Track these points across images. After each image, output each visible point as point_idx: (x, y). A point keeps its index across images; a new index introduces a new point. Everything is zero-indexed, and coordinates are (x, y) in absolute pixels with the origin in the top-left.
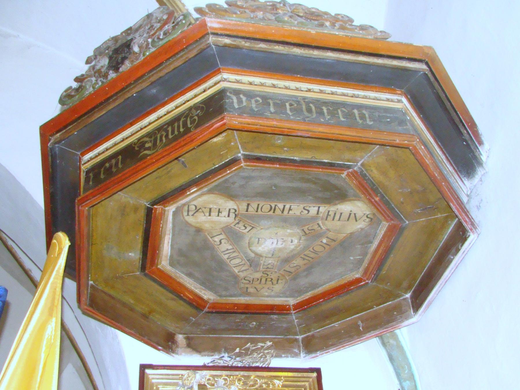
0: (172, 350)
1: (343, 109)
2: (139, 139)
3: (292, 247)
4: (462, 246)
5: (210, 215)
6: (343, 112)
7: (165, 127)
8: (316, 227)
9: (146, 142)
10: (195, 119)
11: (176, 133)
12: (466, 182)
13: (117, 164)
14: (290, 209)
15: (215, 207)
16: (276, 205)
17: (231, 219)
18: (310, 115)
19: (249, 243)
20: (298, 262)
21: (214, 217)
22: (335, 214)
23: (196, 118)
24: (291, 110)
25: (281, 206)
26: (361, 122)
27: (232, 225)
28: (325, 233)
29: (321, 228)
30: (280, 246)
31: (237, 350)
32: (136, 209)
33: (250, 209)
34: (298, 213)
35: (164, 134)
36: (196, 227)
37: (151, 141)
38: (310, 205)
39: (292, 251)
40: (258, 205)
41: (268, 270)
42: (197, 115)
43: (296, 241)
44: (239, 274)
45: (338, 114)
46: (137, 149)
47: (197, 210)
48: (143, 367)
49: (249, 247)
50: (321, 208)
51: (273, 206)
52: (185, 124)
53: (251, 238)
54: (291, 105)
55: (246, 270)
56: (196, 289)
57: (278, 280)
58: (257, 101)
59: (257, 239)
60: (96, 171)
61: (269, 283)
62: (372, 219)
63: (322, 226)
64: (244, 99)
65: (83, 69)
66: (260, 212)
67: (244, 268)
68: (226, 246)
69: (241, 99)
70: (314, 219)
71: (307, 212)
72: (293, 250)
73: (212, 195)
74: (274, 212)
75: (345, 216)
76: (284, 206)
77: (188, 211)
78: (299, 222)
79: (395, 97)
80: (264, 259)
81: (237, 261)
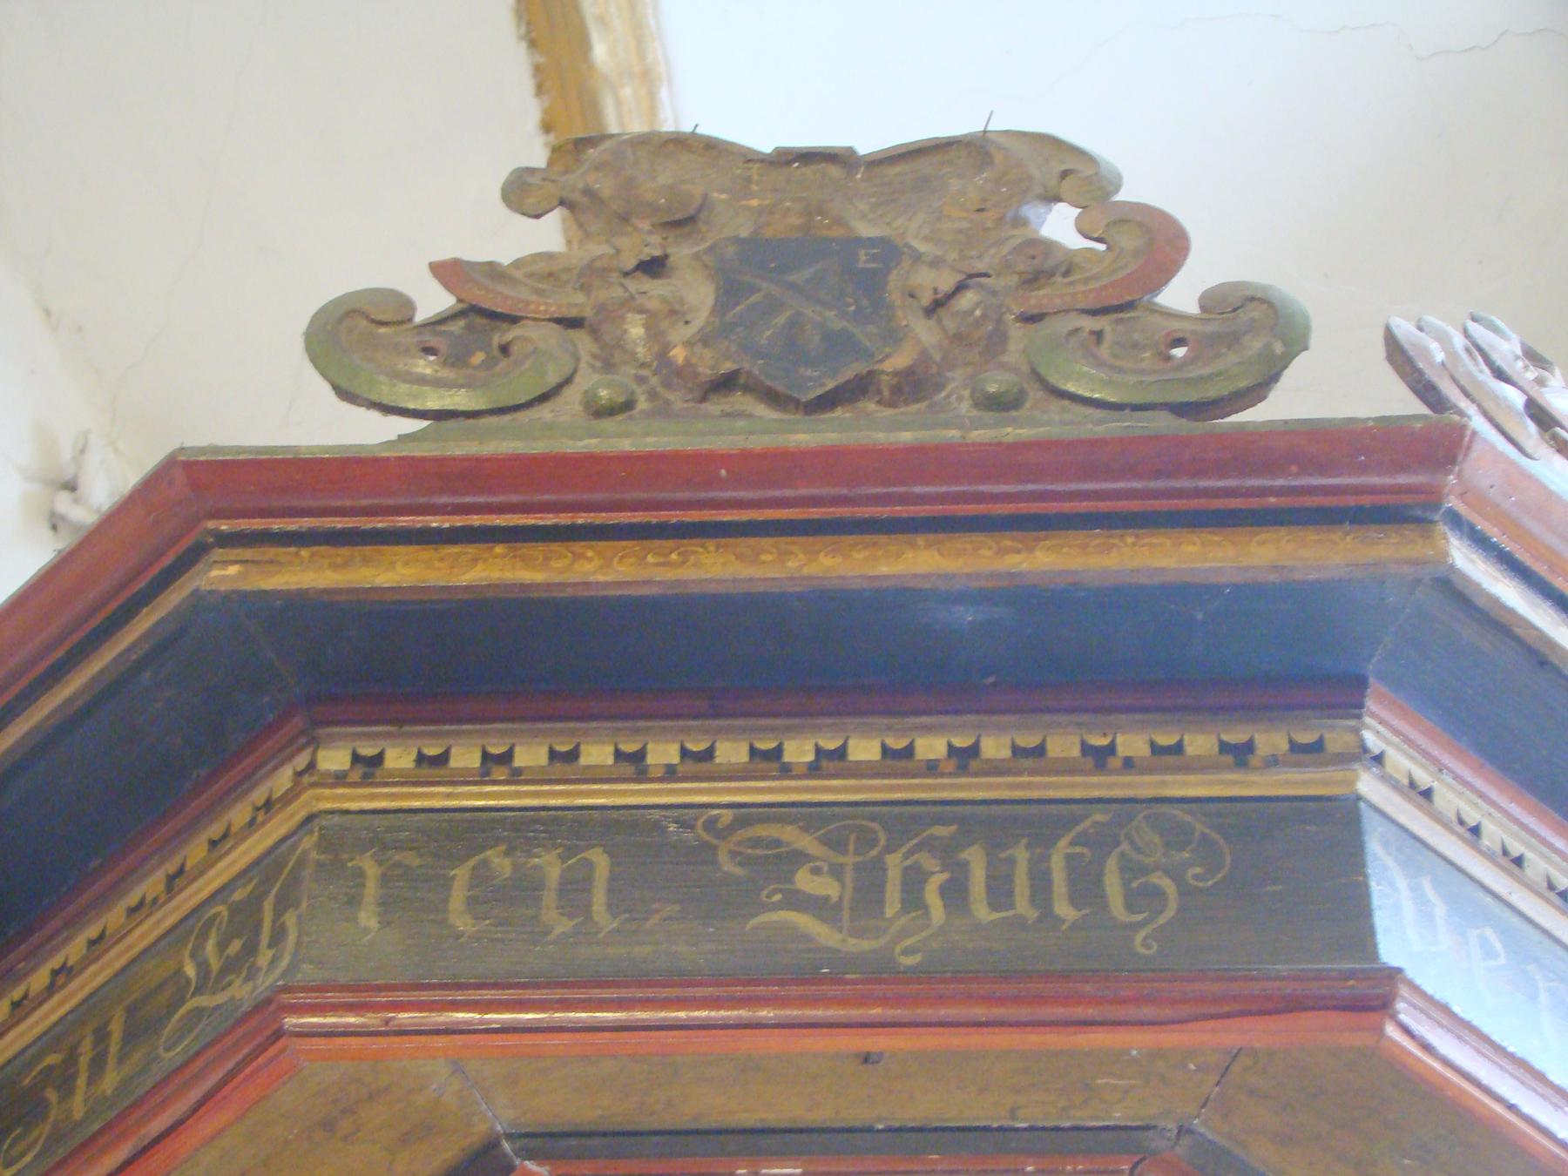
2: (747, 815)
9: (798, 858)
10: (1159, 893)
37: (837, 872)
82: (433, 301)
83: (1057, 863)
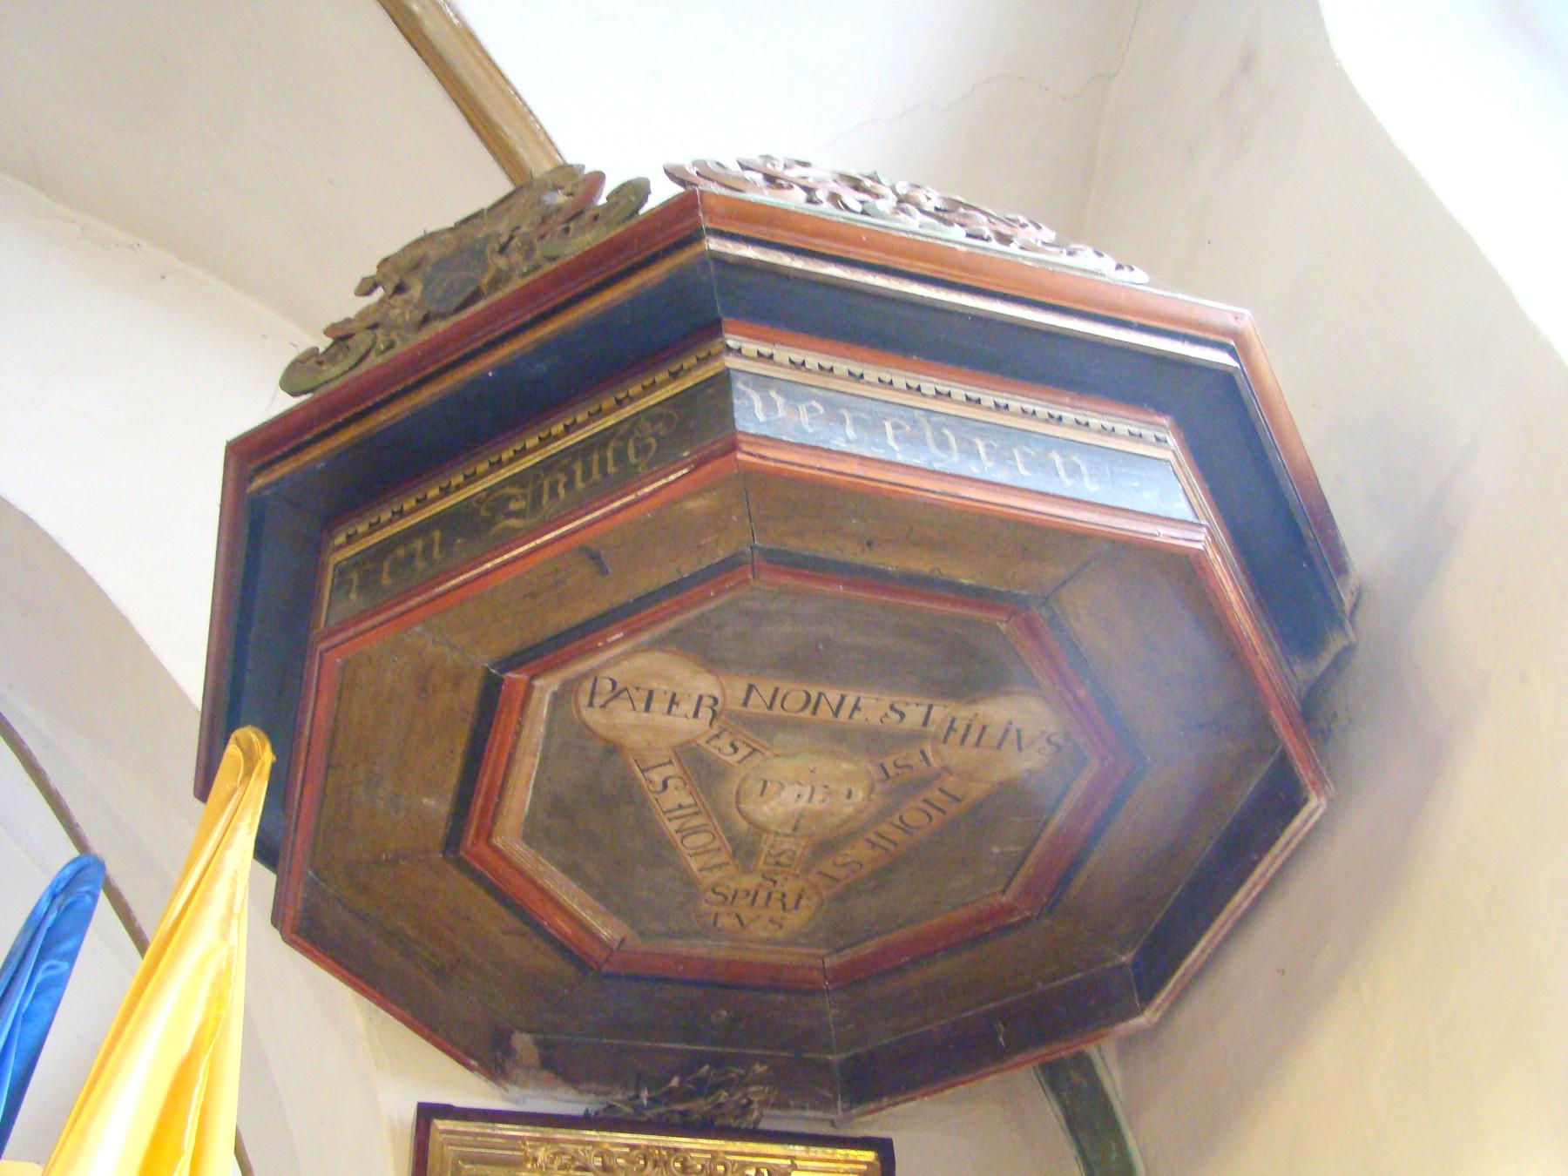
0: (503, 1071)
1: (1027, 450)
3: (849, 810)
4: (1283, 829)
5: (647, 709)
6: (1024, 454)
7: (565, 462)
8: (915, 758)
9: (509, 498)
11: (596, 475)
12: (1297, 670)
13: (428, 550)
14: (856, 707)
15: (665, 687)
16: (820, 695)
17: (700, 725)
18: (944, 456)
19: (738, 793)
20: (858, 852)
21: (658, 716)
22: (969, 726)
23: (653, 441)
24: (896, 438)
25: (833, 696)
26: (1069, 482)
27: (701, 741)
28: (938, 775)
29: (929, 764)
30: (817, 805)
31: (675, 1082)
32: (458, 679)
33: (755, 699)
34: (874, 720)
35: (563, 479)
36: (606, 740)
37: (525, 497)
38: (909, 700)
39: (845, 822)
40: (777, 690)
41: (778, 869)
42: (656, 436)
43: (859, 795)
44: (699, 875)
45: (1013, 458)
46: (483, 513)
47: (617, 692)
48: (427, 1113)
49: (737, 802)
50: (935, 709)
51: (814, 695)
52: (620, 456)
53: (744, 779)
54: (896, 427)
55: (720, 866)
56: (584, 909)
57: (800, 897)
58: (811, 410)
59: (761, 784)
60: (369, 566)
61: (775, 904)
62: (1059, 748)
63: (932, 759)
64: (780, 401)
65: (351, 306)
66: (777, 710)
67: (716, 861)
68: (678, 796)
69: (772, 400)
70: (913, 737)
71: (897, 717)
72: (850, 818)
73: (658, 655)
74: (814, 712)
75: (994, 732)
76: (843, 698)
77: (593, 694)
78: (874, 742)
79: (1149, 434)
80: (772, 837)
81: (702, 839)
82: (324, 343)
83: (610, 454)
